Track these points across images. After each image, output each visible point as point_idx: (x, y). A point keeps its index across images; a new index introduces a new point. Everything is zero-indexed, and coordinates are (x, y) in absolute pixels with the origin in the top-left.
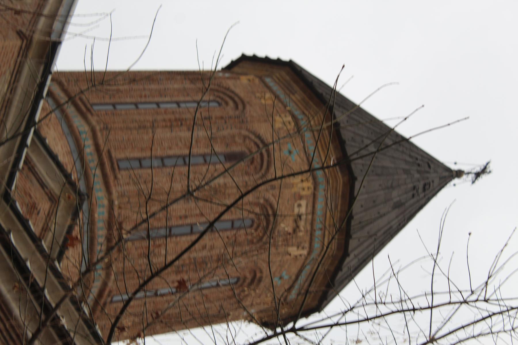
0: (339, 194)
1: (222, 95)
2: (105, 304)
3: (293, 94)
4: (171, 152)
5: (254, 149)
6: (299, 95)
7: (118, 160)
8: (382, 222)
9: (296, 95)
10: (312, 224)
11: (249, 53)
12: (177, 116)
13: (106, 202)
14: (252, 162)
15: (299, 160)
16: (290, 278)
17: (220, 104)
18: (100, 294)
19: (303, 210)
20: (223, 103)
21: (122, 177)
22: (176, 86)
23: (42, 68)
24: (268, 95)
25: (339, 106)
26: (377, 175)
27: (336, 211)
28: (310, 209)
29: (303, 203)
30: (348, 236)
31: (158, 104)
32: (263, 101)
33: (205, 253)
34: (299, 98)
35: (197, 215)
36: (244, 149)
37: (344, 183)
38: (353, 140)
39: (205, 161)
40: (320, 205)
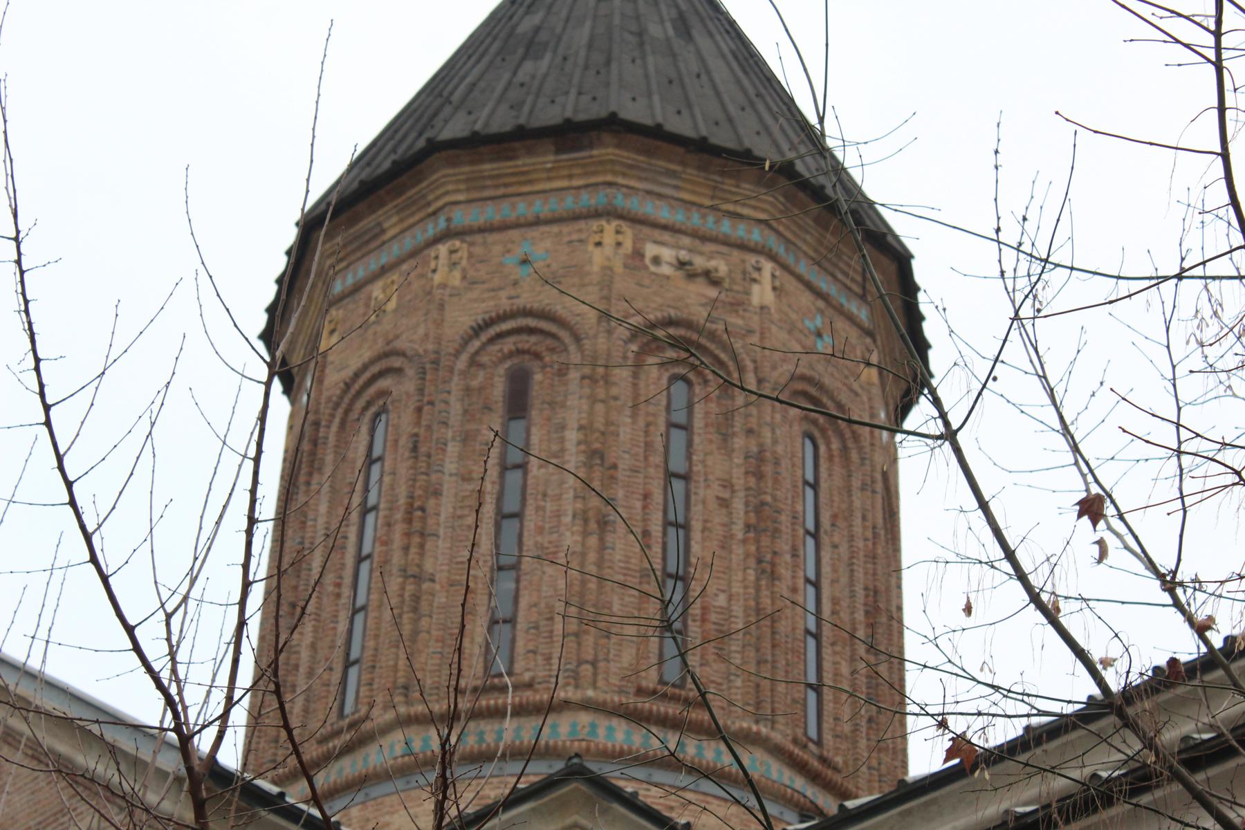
0: (642, 162)
2: (823, 760)
3: (383, 231)
5: (509, 344)
6: (388, 218)
8: (720, 71)
9: (386, 225)
10: (704, 238)
12: (399, 516)
13: (584, 718)
14: (537, 356)
15: (548, 244)
16: (821, 312)
17: (384, 410)
18: (800, 767)
19: (667, 254)
21: (528, 670)
22: (323, 508)
24: (377, 290)
25: (429, 124)
26: (608, 63)
27: (683, 176)
28: (667, 236)
29: (651, 250)
30: (747, 158)
31: (360, 559)
32: (392, 305)
33: (738, 505)
34: (394, 219)
35: (645, 507)
36: (501, 370)
37: (618, 146)
38: (516, 106)
39: (517, 466)
40: (664, 213)
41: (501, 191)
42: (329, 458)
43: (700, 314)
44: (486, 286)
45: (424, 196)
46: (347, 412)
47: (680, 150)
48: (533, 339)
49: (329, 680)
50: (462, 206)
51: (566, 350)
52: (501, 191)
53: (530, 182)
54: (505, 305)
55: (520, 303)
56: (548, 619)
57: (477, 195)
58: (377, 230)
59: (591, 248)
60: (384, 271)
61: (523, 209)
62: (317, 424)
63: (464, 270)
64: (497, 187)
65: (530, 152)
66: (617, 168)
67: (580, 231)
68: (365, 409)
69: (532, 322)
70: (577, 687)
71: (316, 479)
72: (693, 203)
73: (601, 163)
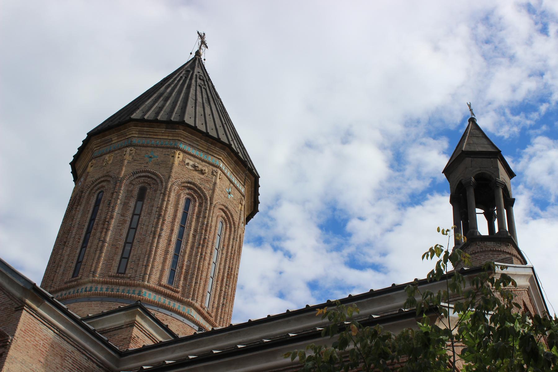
0: (190, 136)
1: (96, 188)
3: (112, 141)
4: (124, 235)
7: (118, 272)
9: (113, 139)
10: (203, 161)
11: (71, 159)
21: (129, 273)
22: (79, 216)
23: (46, 302)
24: (107, 157)
28: (192, 158)
30: (218, 140)
32: (110, 162)
34: (116, 138)
41: (148, 136)
42: (84, 202)
43: (198, 182)
44: (139, 162)
45: (126, 133)
46: (91, 190)
48: (149, 180)
49: (72, 266)
50: (136, 138)
51: (158, 184)
52: (148, 136)
53: (157, 135)
54: (143, 168)
55: (147, 169)
56: (138, 260)
58: (110, 140)
59: (170, 157)
60: (110, 152)
62: (82, 192)
63: (133, 156)
64: (147, 135)
66: (182, 136)
67: (168, 152)
68: (97, 190)
69: (150, 175)
70: (143, 281)
72: (202, 150)
73: (178, 134)
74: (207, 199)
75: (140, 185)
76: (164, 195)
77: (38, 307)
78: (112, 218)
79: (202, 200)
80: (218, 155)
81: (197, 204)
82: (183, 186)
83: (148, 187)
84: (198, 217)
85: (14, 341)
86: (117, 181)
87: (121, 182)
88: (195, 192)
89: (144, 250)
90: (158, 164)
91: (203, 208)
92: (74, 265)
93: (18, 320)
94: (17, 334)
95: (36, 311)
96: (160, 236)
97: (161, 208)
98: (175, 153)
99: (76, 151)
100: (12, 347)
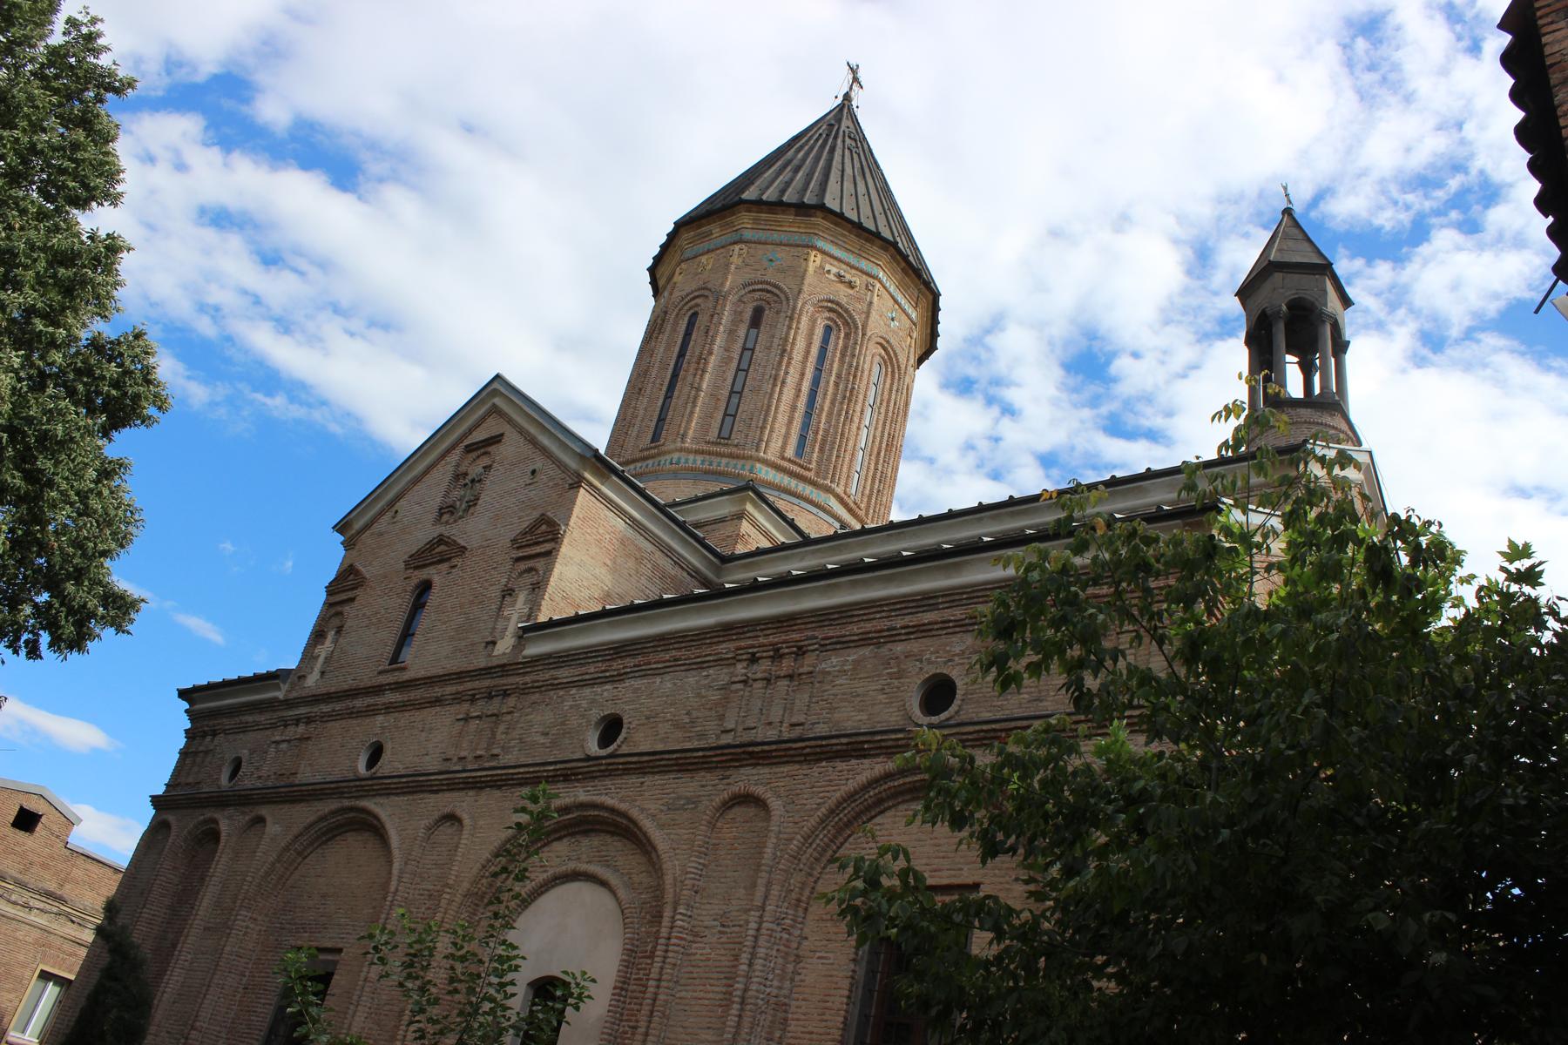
1: (686, 308)
3: (712, 234)
5: (757, 295)
6: (715, 229)
7: (719, 437)
10: (852, 267)
11: (650, 262)
14: (769, 303)
20: (696, 309)
22: (662, 350)
23: (614, 478)
24: (704, 259)
28: (836, 263)
30: (877, 235)
41: (768, 227)
42: (669, 329)
43: (844, 301)
46: (680, 310)
47: (850, 226)
48: (768, 295)
52: (768, 227)
55: (766, 278)
57: (755, 226)
60: (709, 251)
61: (775, 236)
62: (666, 313)
65: (784, 213)
68: (688, 311)
69: (769, 288)
71: (661, 336)
74: (857, 328)
75: (755, 304)
76: (791, 319)
77: (603, 484)
78: (710, 353)
79: (850, 328)
80: (877, 259)
81: (842, 335)
82: (821, 307)
83: (766, 307)
84: (843, 355)
85: (568, 533)
86: (719, 297)
87: (725, 298)
88: (840, 315)
89: (759, 404)
90: (781, 271)
91: (852, 342)
92: (653, 424)
93: (573, 502)
94: (572, 523)
95: (598, 490)
96: (783, 383)
97: (786, 340)
98: (808, 254)
99: (656, 250)
100: (566, 541)
